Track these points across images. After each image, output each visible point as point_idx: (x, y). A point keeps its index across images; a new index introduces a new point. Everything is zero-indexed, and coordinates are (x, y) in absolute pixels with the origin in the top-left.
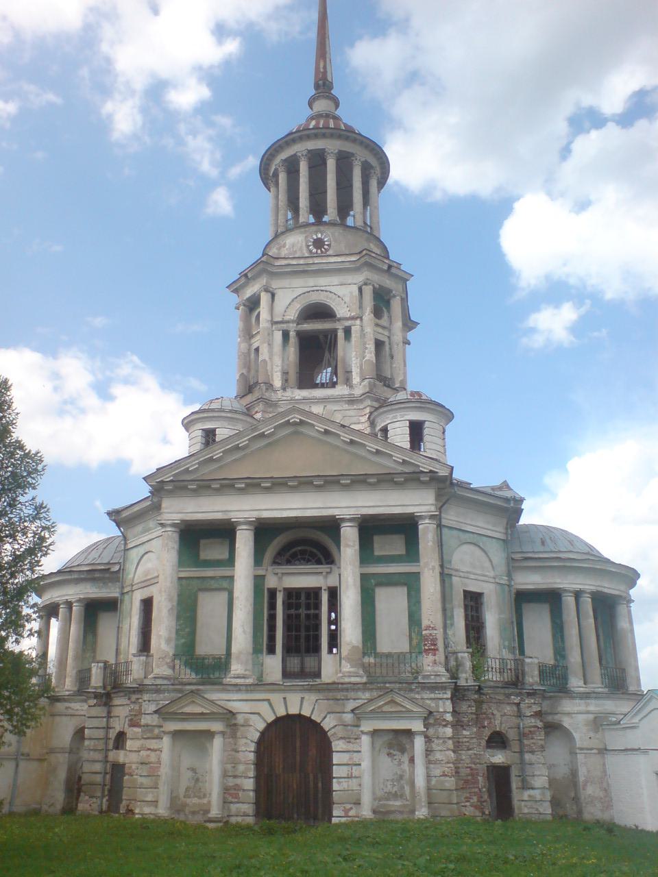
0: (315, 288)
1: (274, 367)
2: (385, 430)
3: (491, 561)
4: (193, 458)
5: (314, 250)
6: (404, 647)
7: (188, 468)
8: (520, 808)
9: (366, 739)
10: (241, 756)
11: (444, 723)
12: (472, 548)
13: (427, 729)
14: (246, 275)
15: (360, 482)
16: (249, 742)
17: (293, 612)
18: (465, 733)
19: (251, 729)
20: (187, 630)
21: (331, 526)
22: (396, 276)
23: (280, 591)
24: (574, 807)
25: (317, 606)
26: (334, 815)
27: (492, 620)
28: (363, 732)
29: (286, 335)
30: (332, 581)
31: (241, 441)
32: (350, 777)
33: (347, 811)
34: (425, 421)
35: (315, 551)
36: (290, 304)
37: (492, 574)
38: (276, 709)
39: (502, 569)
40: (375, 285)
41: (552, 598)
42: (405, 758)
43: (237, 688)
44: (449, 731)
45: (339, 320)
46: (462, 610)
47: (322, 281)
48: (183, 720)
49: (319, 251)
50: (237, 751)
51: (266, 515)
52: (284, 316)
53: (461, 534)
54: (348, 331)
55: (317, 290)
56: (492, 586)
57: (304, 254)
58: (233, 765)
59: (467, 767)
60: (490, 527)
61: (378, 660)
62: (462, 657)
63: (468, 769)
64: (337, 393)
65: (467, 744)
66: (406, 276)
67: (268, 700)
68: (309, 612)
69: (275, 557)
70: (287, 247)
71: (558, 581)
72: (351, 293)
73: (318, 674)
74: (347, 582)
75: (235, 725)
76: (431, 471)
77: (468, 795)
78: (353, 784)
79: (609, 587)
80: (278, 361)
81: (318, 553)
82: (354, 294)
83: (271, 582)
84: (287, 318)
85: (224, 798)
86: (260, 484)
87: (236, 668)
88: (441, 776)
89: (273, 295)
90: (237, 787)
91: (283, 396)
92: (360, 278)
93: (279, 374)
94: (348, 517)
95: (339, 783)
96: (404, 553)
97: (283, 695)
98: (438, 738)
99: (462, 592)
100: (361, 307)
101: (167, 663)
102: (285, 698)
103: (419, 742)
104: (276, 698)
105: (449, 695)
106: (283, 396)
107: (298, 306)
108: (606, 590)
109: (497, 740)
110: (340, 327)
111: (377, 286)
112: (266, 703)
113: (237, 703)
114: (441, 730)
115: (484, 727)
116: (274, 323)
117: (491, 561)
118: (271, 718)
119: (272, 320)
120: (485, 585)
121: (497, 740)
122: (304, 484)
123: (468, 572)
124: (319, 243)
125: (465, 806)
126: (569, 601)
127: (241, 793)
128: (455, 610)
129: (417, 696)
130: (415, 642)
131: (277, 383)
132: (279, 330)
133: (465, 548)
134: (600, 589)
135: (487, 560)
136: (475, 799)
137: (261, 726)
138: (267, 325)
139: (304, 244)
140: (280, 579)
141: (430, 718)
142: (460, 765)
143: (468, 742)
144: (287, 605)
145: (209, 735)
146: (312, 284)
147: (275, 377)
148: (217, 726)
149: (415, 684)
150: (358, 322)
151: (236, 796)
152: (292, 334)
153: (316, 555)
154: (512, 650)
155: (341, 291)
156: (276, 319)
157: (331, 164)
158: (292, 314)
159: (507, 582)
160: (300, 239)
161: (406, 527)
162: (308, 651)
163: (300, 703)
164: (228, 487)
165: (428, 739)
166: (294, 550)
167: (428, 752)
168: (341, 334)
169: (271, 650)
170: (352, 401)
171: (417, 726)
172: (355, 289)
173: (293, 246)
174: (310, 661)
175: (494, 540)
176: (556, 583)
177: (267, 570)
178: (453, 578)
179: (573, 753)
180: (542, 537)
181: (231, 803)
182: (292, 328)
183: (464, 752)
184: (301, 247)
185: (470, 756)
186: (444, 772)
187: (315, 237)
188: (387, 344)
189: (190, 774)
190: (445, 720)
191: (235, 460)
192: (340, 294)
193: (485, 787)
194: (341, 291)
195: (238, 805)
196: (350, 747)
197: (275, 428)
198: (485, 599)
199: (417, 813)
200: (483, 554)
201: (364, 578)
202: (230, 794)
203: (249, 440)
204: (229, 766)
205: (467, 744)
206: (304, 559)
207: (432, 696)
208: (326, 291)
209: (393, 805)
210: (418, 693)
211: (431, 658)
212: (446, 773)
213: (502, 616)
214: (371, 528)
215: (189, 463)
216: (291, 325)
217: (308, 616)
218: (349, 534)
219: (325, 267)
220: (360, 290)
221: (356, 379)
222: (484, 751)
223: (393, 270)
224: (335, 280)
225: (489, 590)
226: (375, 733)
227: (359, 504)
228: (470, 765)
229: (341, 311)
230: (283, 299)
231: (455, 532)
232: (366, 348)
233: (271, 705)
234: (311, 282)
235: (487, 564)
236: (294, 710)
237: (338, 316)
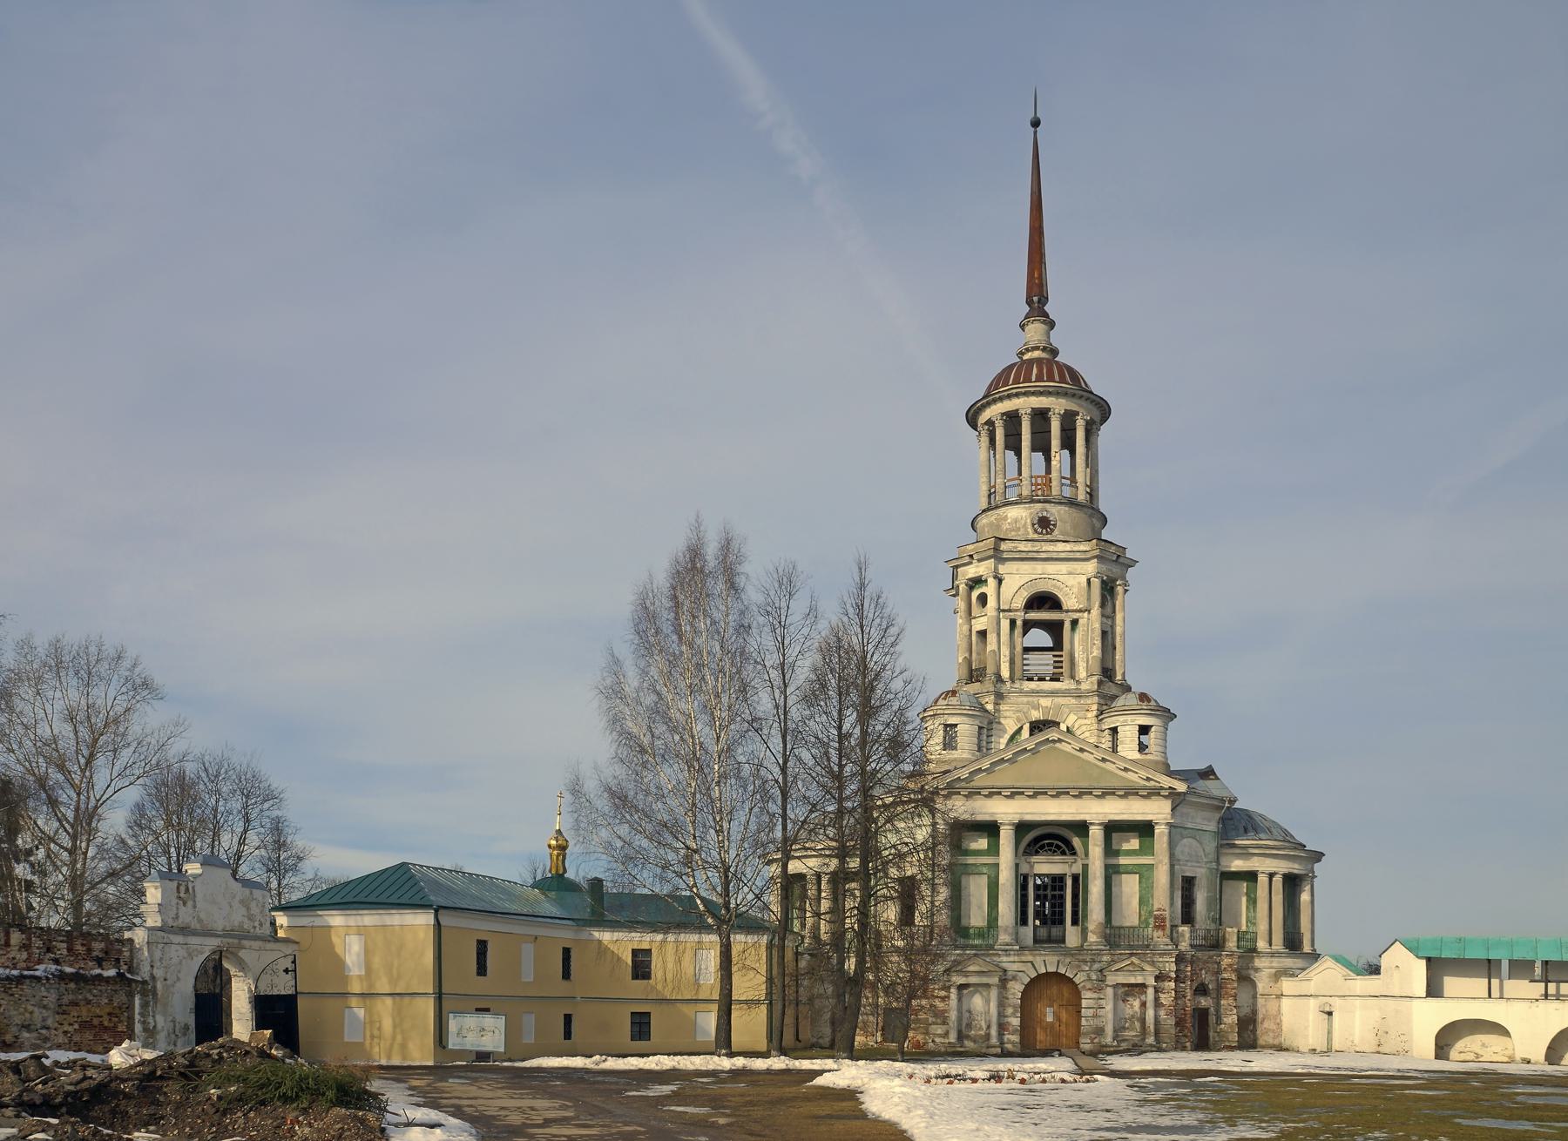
1: (1002, 657)
2: (1114, 730)
3: (1204, 850)
5: (1039, 530)
6: (1136, 923)
8: (1214, 1038)
9: (1110, 991)
12: (1190, 840)
14: (971, 556)
17: (1041, 892)
21: (1082, 828)
22: (1123, 564)
24: (1252, 1036)
25: (1062, 888)
27: (1201, 898)
28: (1107, 986)
29: (1013, 623)
30: (1077, 869)
32: (1095, 1016)
33: (1092, 1039)
34: (1152, 726)
35: (1060, 844)
38: (1038, 969)
39: (1212, 856)
42: (1137, 1004)
44: (1172, 984)
45: (1067, 611)
47: (1051, 568)
51: (1028, 818)
54: (1075, 623)
56: (1203, 871)
57: (1028, 534)
61: (1112, 931)
62: (1183, 930)
64: (1064, 687)
66: (1126, 562)
67: (1031, 962)
68: (1055, 893)
69: (1029, 845)
70: (1009, 521)
72: (1079, 583)
73: (1063, 941)
74: (1095, 874)
78: (1097, 1022)
79: (1296, 868)
80: (1005, 651)
81: (1062, 845)
83: (1024, 869)
84: (1014, 606)
85: (999, 1031)
87: (1004, 938)
89: (1000, 581)
91: (1011, 687)
93: (1008, 664)
95: (1087, 1021)
96: (1138, 848)
97: (1044, 958)
100: (1089, 599)
103: (1150, 991)
104: (1038, 961)
105: (1174, 960)
107: (1024, 595)
109: (1202, 990)
110: (1067, 620)
111: (1105, 578)
113: (1011, 963)
114: (1166, 984)
116: (999, 610)
117: (1204, 850)
118: (1034, 975)
119: (999, 608)
120: (1198, 870)
121: (1202, 990)
122: (1060, 793)
123: (1187, 861)
124: (1044, 523)
130: (1143, 918)
131: (1005, 673)
133: (1185, 840)
137: (1027, 980)
138: (995, 613)
139: (1028, 521)
141: (1159, 978)
144: (1037, 887)
147: (1002, 667)
149: (1142, 949)
150: (1086, 614)
152: (1019, 623)
153: (1061, 847)
154: (1214, 921)
155: (1071, 581)
156: (1007, 607)
158: (1019, 602)
159: (1215, 867)
160: (1024, 515)
161: (1144, 829)
162: (1054, 923)
163: (1047, 962)
164: (994, 793)
165: (1157, 990)
166: (1042, 843)
167: (1157, 999)
168: (1067, 626)
169: (1024, 922)
170: (1079, 695)
172: (1084, 579)
173: (1016, 522)
174: (1055, 931)
178: (1176, 867)
179: (1255, 997)
180: (1244, 824)
182: (1020, 617)
184: (1026, 523)
188: (1110, 633)
189: (968, 1014)
192: (1069, 584)
194: (1071, 581)
196: (1095, 995)
198: (1197, 882)
199: (1147, 1040)
200: (1198, 845)
201: (1107, 867)
204: (1001, 1009)
206: (1050, 850)
207: (1161, 960)
209: (1127, 1036)
211: (1160, 933)
213: (1209, 894)
214: (1113, 829)
216: (1018, 613)
217: (1054, 897)
218: (1096, 833)
219: (1055, 555)
220: (1089, 581)
221: (1082, 673)
223: (1121, 560)
225: (1200, 872)
226: (1116, 986)
229: (1070, 601)
231: (1179, 830)
232: (1094, 644)
233: (1033, 965)
234: (1039, 567)
236: (1052, 969)
237: (1065, 607)
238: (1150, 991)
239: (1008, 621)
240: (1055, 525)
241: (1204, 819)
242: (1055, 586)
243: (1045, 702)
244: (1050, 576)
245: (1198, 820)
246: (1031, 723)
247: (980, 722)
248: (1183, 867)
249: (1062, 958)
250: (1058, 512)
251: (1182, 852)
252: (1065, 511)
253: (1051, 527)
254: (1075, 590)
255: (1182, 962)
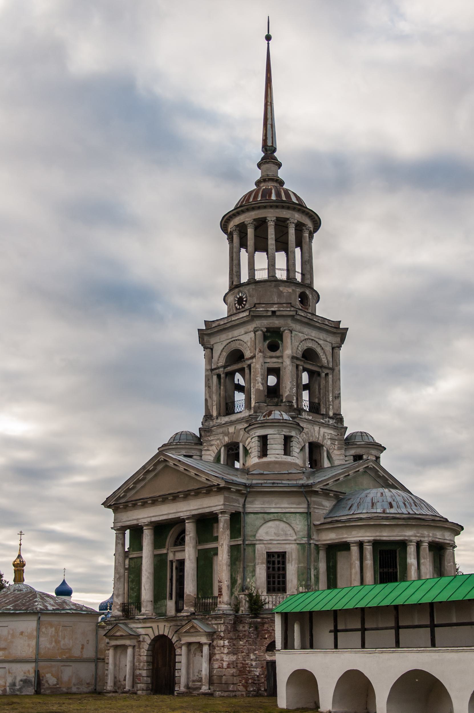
0: (233, 339)
3: (294, 529)
4: (120, 490)
7: (120, 496)
10: (141, 658)
11: (220, 638)
12: (277, 523)
13: (213, 642)
15: (187, 495)
16: (145, 650)
18: (241, 643)
19: (145, 644)
20: (137, 588)
23: (174, 562)
26: (176, 690)
29: (219, 376)
31: (139, 476)
36: (220, 354)
37: (295, 537)
40: (263, 329)
41: (345, 546)
43: (145, 620)
46: (264, 566)
47: (235, 333)
48: (116, 639)
49: (241, 307)
50: (141, 656)
52: (218, 363)
53: (266, 515)
55: (234, 340)
56: (294, 546)
58: (139, 663)
59: (241, 663)
60: (295, 506)
63: (241, 664)
65: (241, 649)
69: (176, 542)
71: (345, 536)
72: (251, 338)
75: (140, 641)
76: (218, 485)
77: (241, 679)
82: (252, 339)
86: (147, 502)
88: (218, 668)
89: (212, 349)
90: (140, 675)
92: (251, 327)
94: (185, 517)
95: (178, 672)
98: (218, 646)
99: (266, 553)
101: (117, 608)
102: (158, 626)
103: (206, 649)
106: (216, 423)
108: (384, 538)
112: (151, 629)
113: (139, 628)
115: (266, 638)
117: (294, 529)
120: (287, 546)
123: (271, 540)
125: (239, 685)
126: (355, 549)
127: (141, 678)
128: (257, 566)
129: (210, 623)
132: (215, 375)
133: (270, 524)
134: (378, 538)
135: (291, 529)
136: (243, 682)
137: (149, 641)
140: (174, 555)
142: (238, 662)
143: (242, 648)
145: (124, 647)
146: (230, 337)
148: (127, 642)
150: (254, 360)
151: (139, 680)
152: (223, 376)
157: (250, 232)
169: (171, 598)
171: (204, 640)
175: (298, 515)
176: (344, 538)
177: (168, 550)
178: (257, 546)
181: (138, 683)
183: (240, 654)
185: (243, 656)
186: (219, 666)
187: (238, 297)
190: (220, 636)
191: (142, 487)
192: (245, 341)
193: (263, 674)
195: (140, 685)
197: (154, 465)
200: (287, 525)
202: (135, 678)
203: (143, 474)
205: (241, 649)
207: (216, 622)
208: (239, 340)
210: (210, 621)
212: (220, 667)
213: (302, 565)
215: (119, 493)
222: (264, 653)
223: (278, 313)
224: (242, 330)
227: (192, 508)
228: (242, 662)
230: (218, 349)
235: (291, 532)
238: (206, 649)
239: (216, 376)
240: (246, 301)
241: (292, 503)
242: (240, 344)
243: (231, 430)
244: (236, 338)
245: (286, 506)
246: (225, 446)
247: (186, 452)
248: (270, 546)
249: (166, 624)
250: (248, 291)
251: (267, 533)
252: (253, 289)
253: (244, 303)
254: (249, 344)
255: (241, 623)
